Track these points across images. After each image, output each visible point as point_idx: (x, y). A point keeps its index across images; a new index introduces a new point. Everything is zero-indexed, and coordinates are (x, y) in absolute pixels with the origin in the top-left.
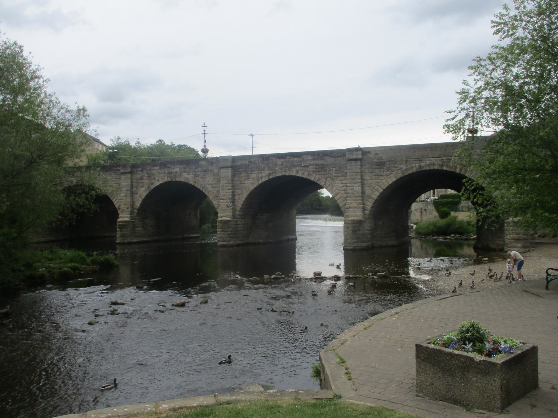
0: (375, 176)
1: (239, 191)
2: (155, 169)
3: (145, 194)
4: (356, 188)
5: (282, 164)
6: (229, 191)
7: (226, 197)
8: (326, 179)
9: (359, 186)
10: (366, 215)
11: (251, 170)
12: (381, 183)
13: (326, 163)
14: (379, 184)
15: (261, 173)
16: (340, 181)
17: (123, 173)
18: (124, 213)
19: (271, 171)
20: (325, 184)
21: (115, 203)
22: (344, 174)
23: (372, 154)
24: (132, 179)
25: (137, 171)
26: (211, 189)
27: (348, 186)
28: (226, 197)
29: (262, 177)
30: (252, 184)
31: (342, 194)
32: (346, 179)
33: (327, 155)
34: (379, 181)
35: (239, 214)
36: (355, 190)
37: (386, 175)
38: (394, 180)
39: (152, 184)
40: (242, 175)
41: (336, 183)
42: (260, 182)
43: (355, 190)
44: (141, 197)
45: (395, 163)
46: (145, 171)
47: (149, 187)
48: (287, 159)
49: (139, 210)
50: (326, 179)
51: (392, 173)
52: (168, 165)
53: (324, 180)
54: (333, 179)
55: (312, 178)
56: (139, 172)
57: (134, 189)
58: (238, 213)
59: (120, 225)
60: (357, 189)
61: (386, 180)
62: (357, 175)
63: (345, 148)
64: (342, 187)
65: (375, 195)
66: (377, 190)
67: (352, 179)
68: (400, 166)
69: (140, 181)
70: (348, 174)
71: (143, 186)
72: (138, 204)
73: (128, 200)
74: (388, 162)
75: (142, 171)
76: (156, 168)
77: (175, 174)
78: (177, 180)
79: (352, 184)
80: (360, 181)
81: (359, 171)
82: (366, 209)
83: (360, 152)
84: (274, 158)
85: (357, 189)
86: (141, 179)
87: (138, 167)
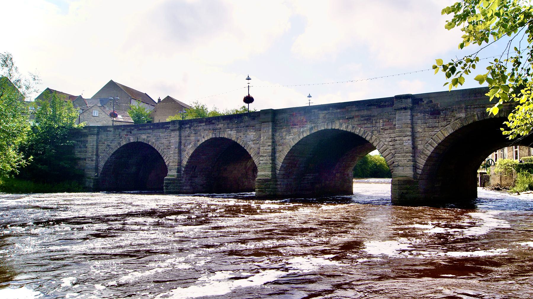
0: (429, 127)
1: (280, 148)
2: (201, 126)
3: (191, 152)
4: (407, 143)
5: (324, 118)
6: (270, 148)
7: (266, 154)
8: (372, 132)
9: (409, 140)
10: (418, 174)
11: (292, 124)
12: (435, 135)
13: (372, 115)
14: (434, 137)
15: (303, 127)
16: (388, 135)
17: (172, 130)
18: (172, 171)
19: (313, 125)
20: (371, 139)
21: (165, 161)
22: (392, 126)
23: (425, 102)
24: (180, 136)
25: (185, 128)
26: (253, 146)
27: (396, 141)
28: (266, 154)
29: (303, 132)
30: (293, 139)
31: (390, 150)
32: (394, 133)
33: (374, 105)
34: (433, 133)
35: (279, 173)
36: (404, 144)
37: (441, 127)
38: (451, 131)
39: (198, 141)
40: (283, 130)
41: (383, 137)
42: (301, 137)
43: (404, 144)
44: (188, 155)
45: (453, 112)
46: (192, 128)
47: (195, 144)
48: (330, 111)
49: (187, 167)
50: (372, 132)
51: (448, 123)
52: (213, 121)
53: (371, 133)
54: (380, 132)
55: (357, 132)
56: (187, 129)
57: (182, 147)
58: (278, 171)
59: (166, 183)
60: (407, 144)
61: (442, 132)
62: (407, 127)
63: (393, 95)
64: (390, 141)
65: (429, 150)
66: (431, 145)
67: (401, 132)
68: (458, 115)
69: (188, 138)
70: (397, 126)
71: (190, 143)
72: (185, 162)
73: (176, 157)
74: (443, 110)
75: (190, 128)
76: (202, 124)
77: (219, 130)
78: (221, 136)
79: (401, 138)
80: (410, 134)
81: (409, 122)
82: (418, 167)
83: (410, 100)
84: (316, 111)
85: (407, 144)
86: (189, 137)
87: (187, 124)
